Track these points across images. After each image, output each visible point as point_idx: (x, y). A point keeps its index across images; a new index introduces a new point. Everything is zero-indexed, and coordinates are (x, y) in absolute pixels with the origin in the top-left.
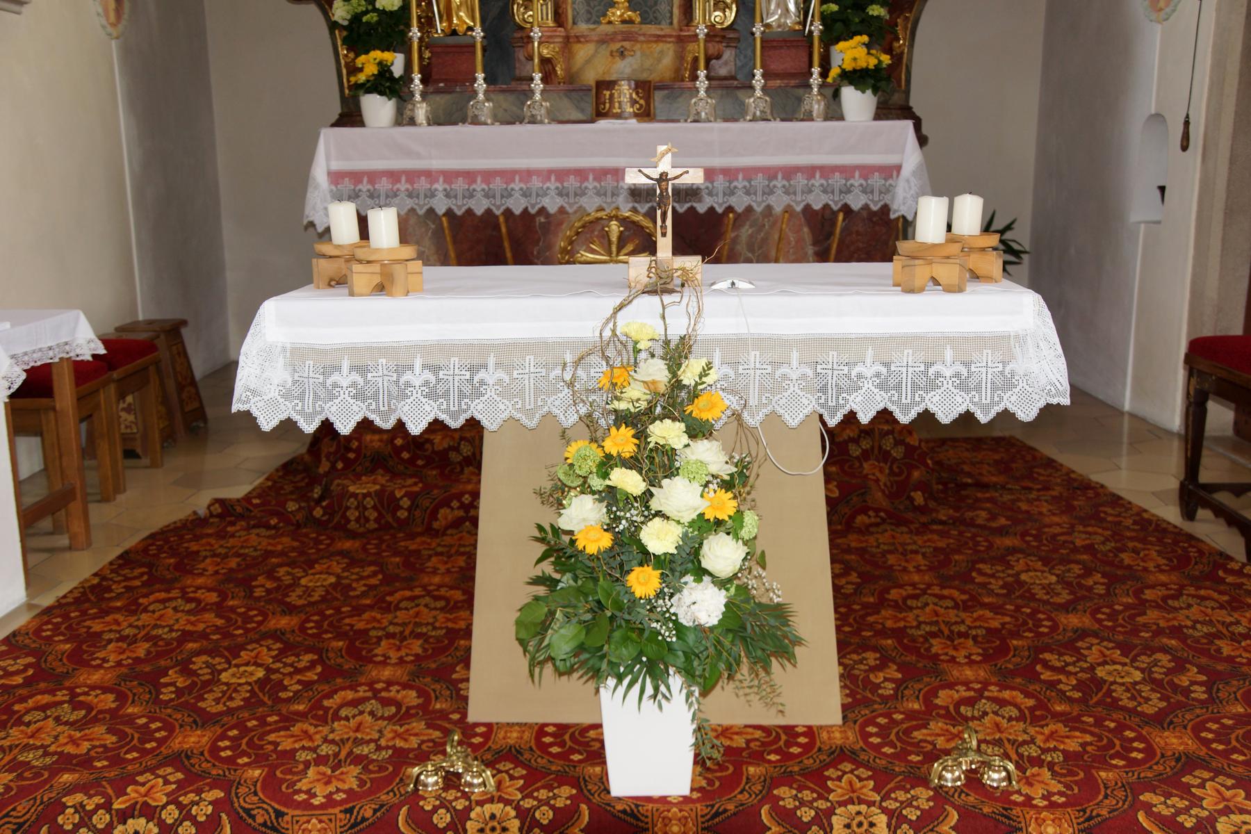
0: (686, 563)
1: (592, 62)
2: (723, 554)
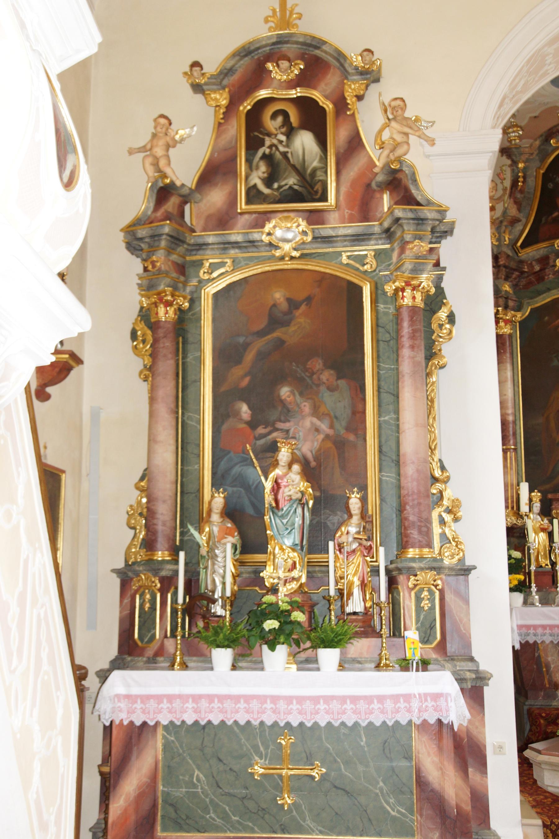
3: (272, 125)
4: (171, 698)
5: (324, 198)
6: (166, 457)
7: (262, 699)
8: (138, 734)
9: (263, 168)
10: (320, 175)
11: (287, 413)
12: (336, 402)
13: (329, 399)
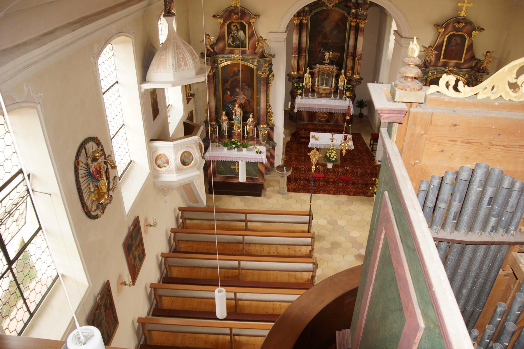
0: (333, 157)
1: (321, 91)
5: (246, 47)
6: (213, 104)
7: (233, 157)
9: (231, 39)
10: (245, 42)
11: (238, 94)
12: (248, 93)
13: (246, 91)
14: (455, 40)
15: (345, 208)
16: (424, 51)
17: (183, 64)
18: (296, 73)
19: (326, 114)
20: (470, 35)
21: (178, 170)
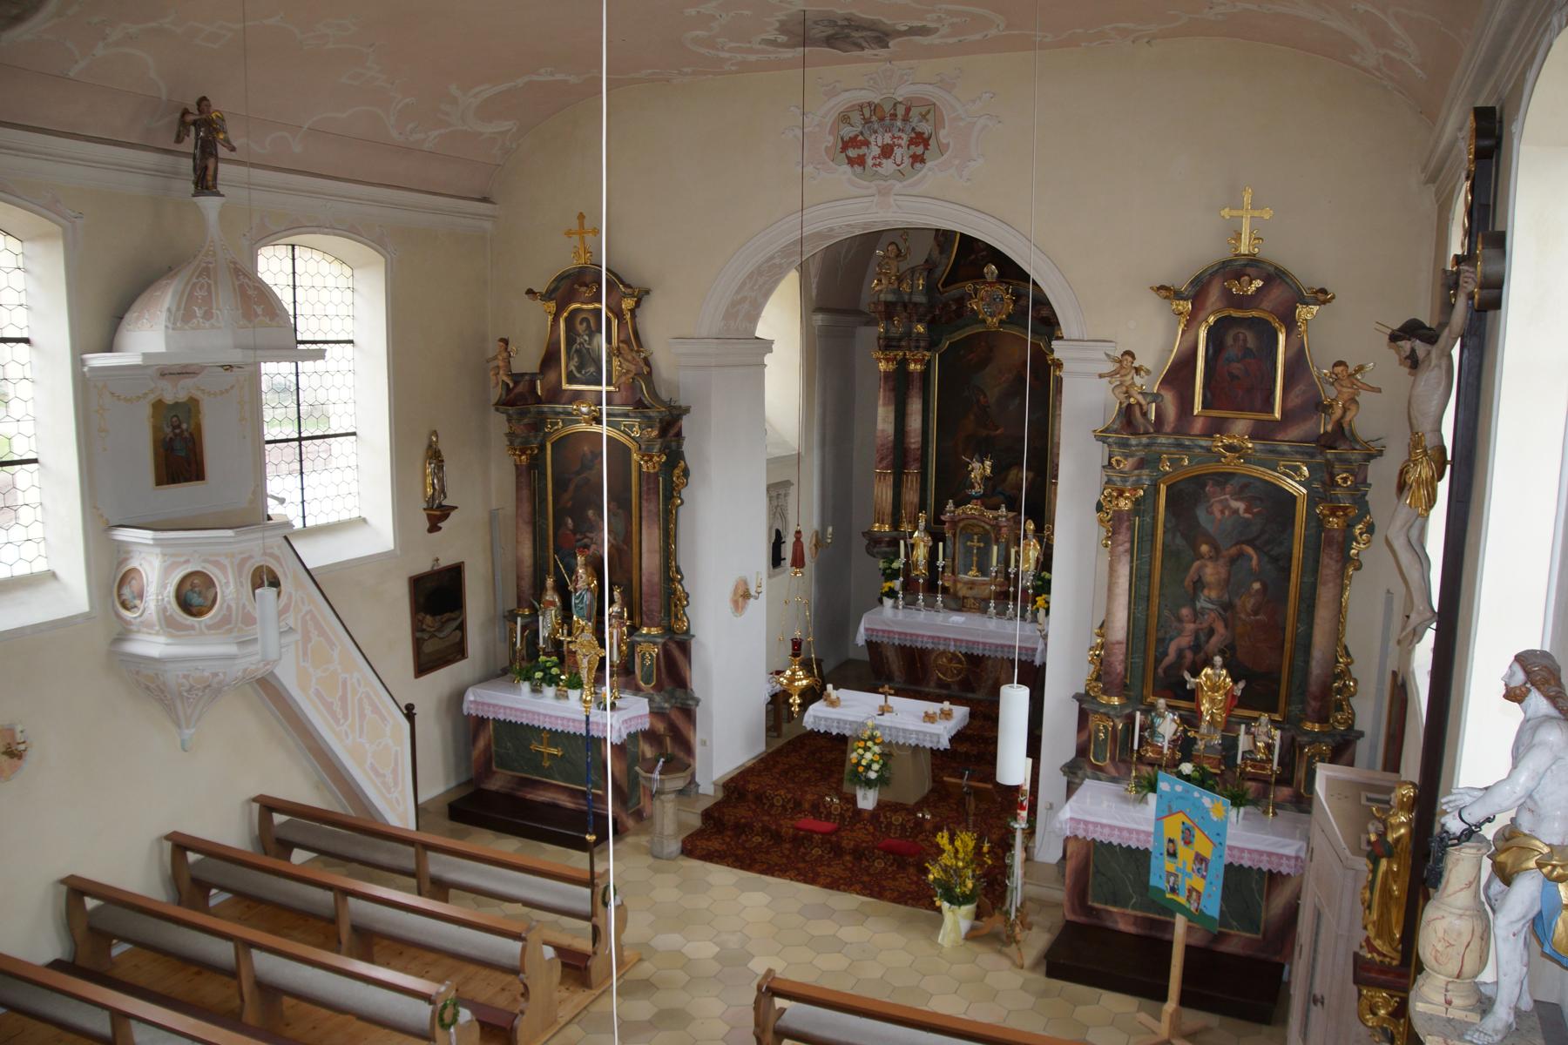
0: (868, 767)
1: (963, 591)
2: (876, 767)
3: (581, 328)
4: (495, 706)
6: (526, 551)
8: (481, 722)
14: (1236, 339)
15: (823, 928)
16: (1111, 375)
17: (199, 313)
18: (887, 528)
19: (960, 662)
20: (1290, 323)
21: (169, 624)
